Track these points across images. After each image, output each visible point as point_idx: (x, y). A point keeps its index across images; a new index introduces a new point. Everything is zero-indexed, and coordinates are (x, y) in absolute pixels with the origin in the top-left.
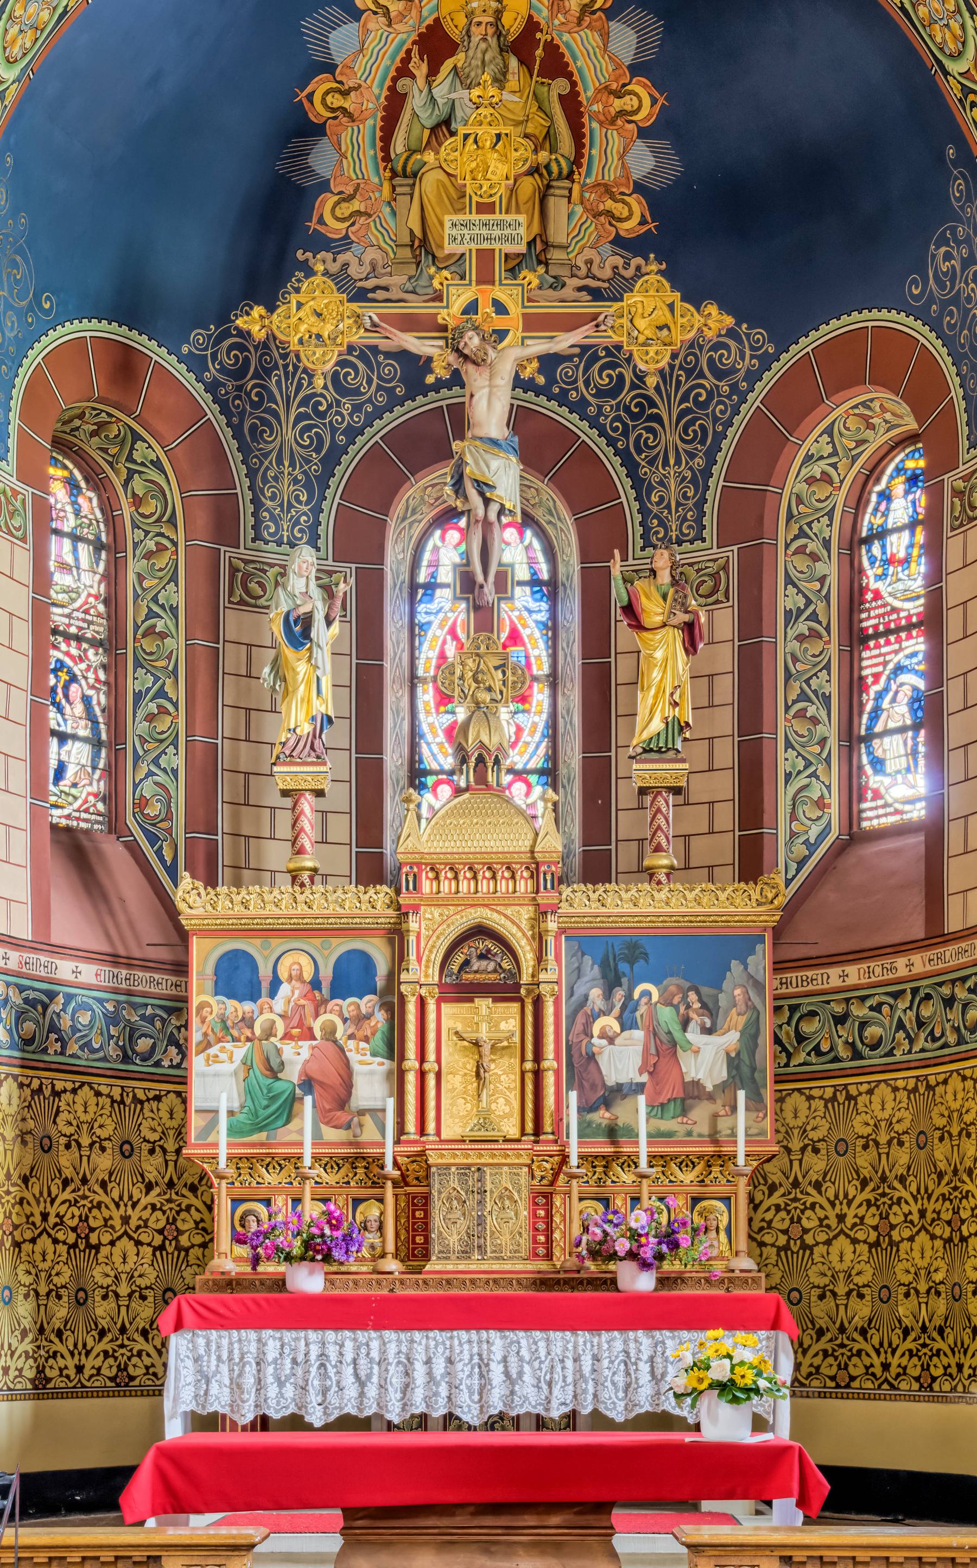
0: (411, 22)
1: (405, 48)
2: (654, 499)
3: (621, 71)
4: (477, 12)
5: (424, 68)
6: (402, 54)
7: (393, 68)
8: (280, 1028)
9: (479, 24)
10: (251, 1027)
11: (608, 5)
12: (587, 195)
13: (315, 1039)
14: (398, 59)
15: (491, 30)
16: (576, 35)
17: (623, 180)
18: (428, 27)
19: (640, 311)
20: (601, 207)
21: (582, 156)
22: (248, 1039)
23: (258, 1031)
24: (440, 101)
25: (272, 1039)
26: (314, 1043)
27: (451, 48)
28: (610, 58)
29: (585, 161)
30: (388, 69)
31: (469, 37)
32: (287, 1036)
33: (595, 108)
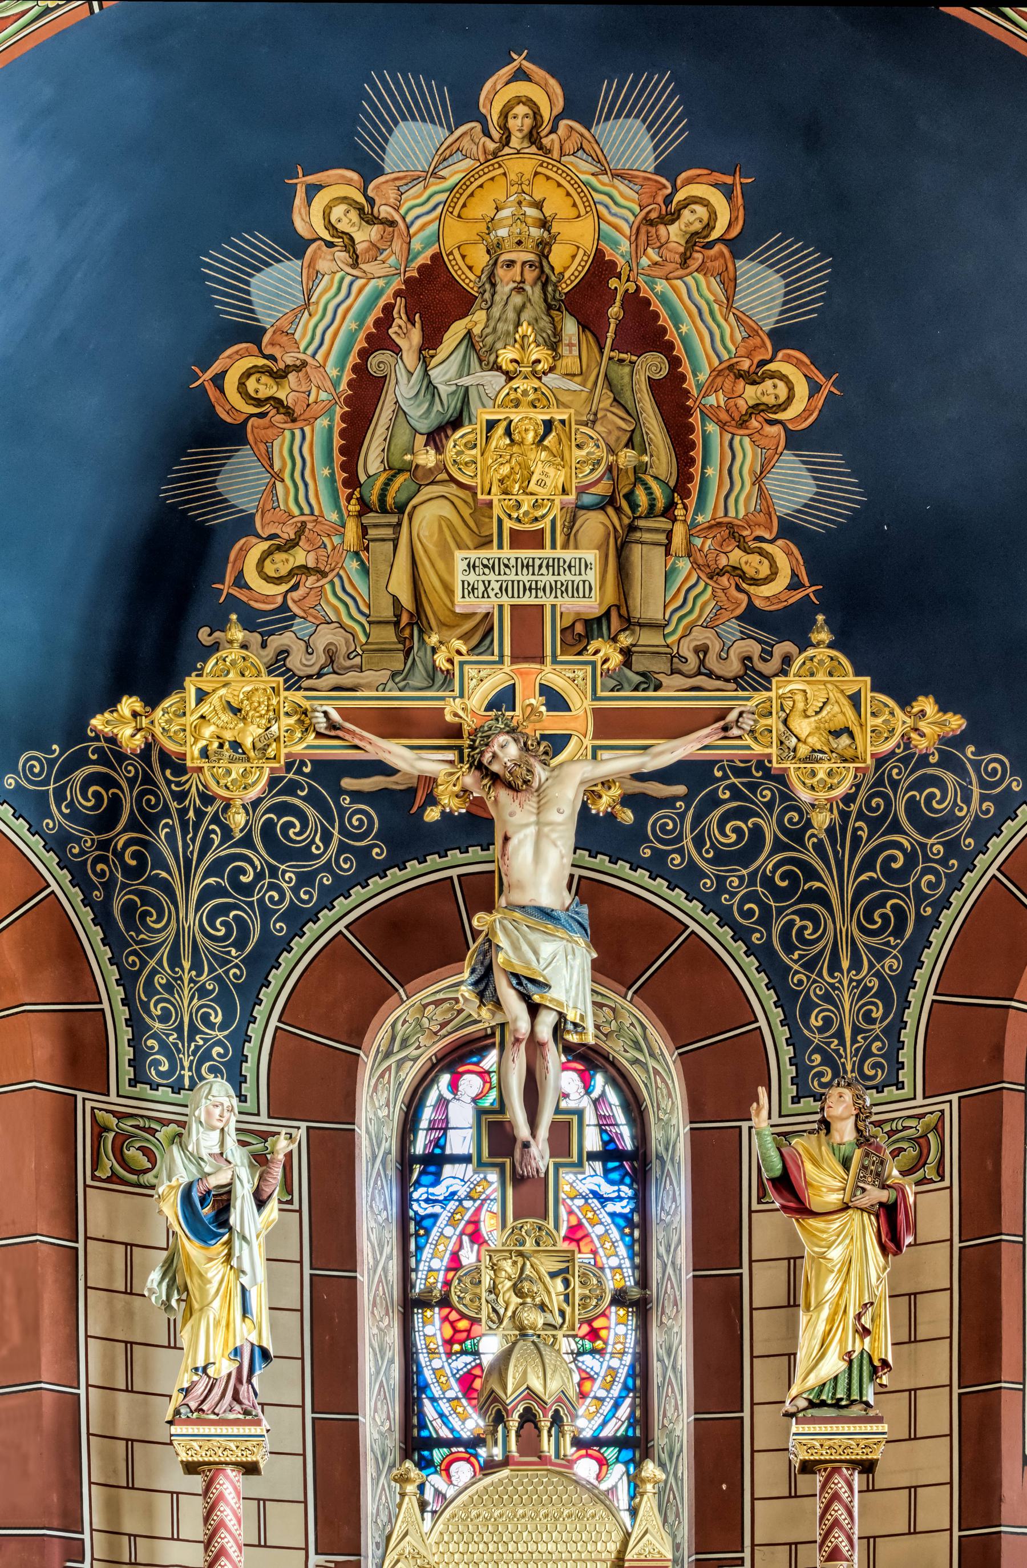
2: (816, 1022)
12: (698, 542)
17: (762, 518)
19: (800, 705)
20: (723, 561)
21: (690, 478)
29: (694, 487)
33: (712, 400)
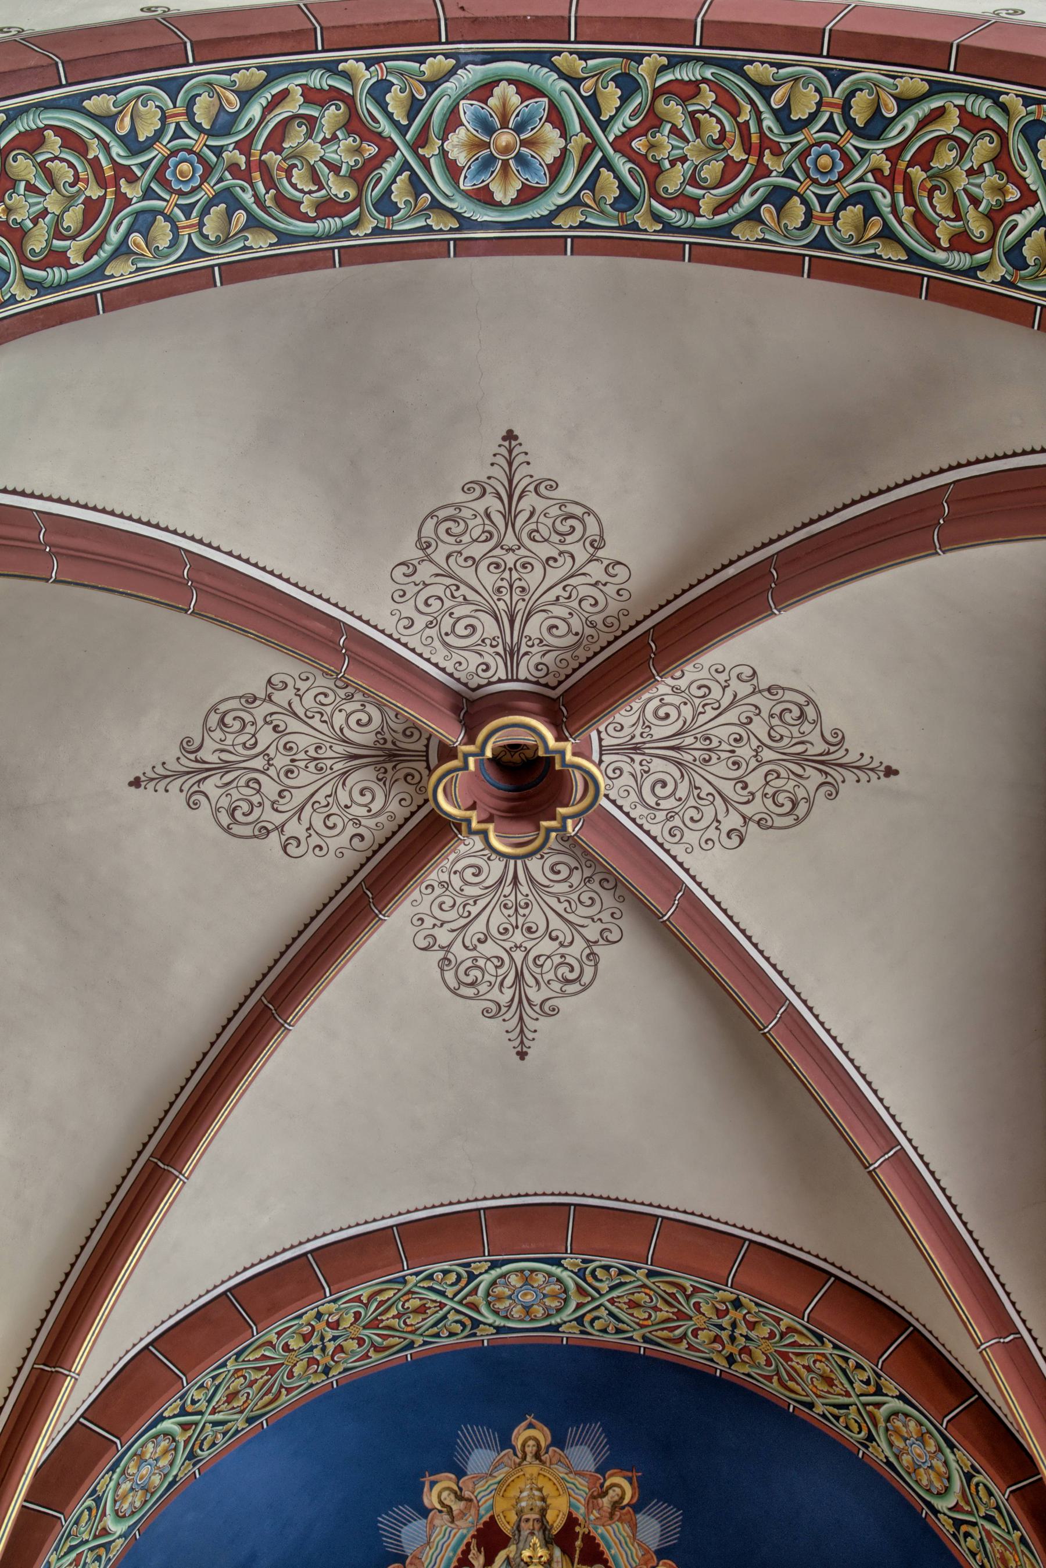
0: (470, 1519)
1: (465, 1542)
3: (648, 1556)
4: (526, 1510)
5: (482, 1559)
6: (463, 1547)
7: (455, 1559)
9: (527, 1520)
11: (635, 1500)
14: (459, 1551)
15: (537, 1526)
16: (609, 1528)
18: (485, 1523)
27: (504, 1541)
28: (639, 1545)
30: (450, 1560)
31: (519, 1531)
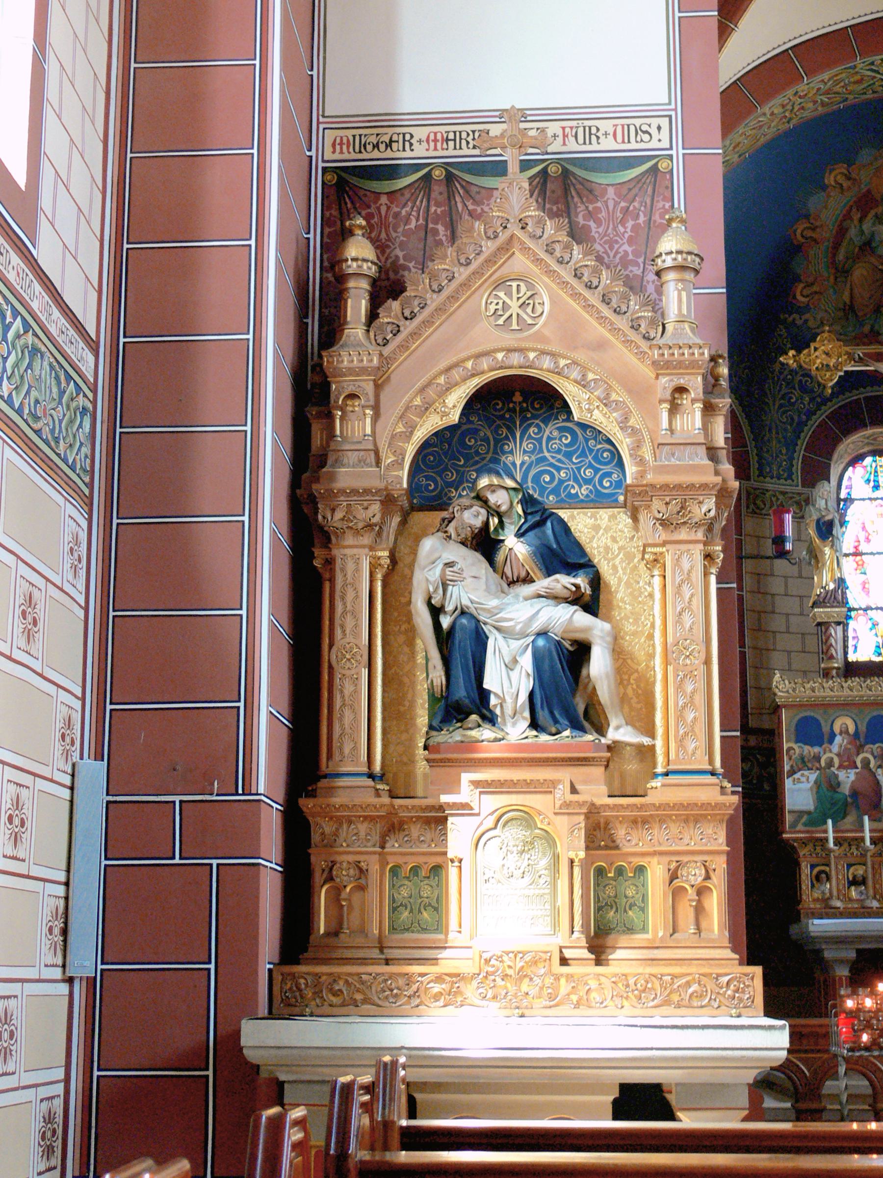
8: (836, 761)
10: (819, 761)
13: (857, 768)
22: (817, 769)
23: (823, 763)
24: (866, 232)
25: (832, 769)
26: (857, 771)
32: (841, 767)
